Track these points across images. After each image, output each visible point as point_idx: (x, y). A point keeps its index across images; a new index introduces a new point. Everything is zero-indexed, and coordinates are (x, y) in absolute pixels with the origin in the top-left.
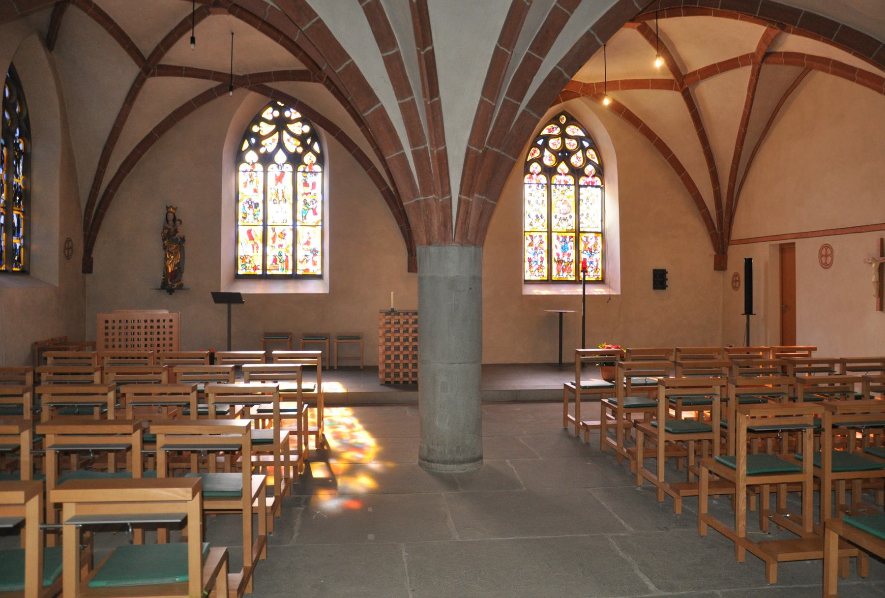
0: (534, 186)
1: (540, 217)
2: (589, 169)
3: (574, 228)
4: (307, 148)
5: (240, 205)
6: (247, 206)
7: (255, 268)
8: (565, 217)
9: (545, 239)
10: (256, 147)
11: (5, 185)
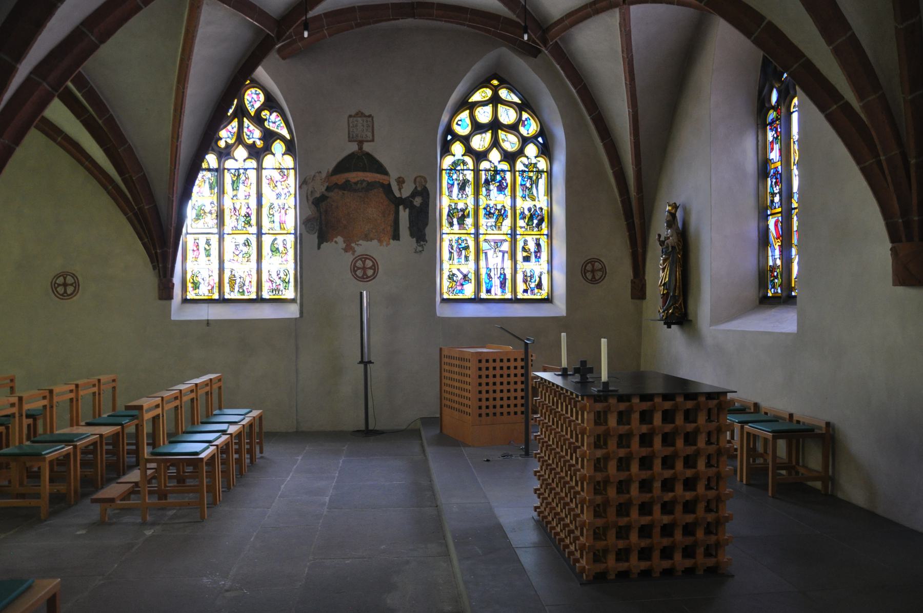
5: (769, 179)
6: (774, 180)
11: (509, 212)
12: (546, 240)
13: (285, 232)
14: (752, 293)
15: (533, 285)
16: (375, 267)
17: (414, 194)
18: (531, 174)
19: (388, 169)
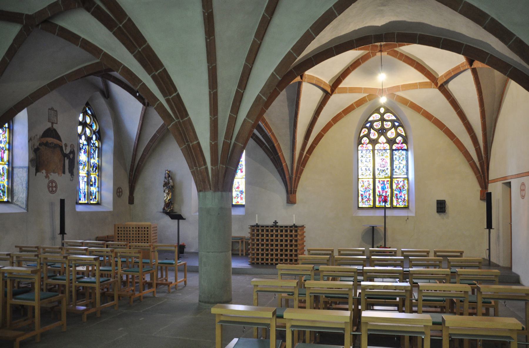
0: (364, 152)
1: (368, 170)
2: (399, 139)
3: (389, 175)
8: (384, 169)
9: (371, 183)
11: (87, 163)
12: (97, 177)
13: (4, 163)
15: (94, 197)
18: (94, 148)
19: (62, 139)
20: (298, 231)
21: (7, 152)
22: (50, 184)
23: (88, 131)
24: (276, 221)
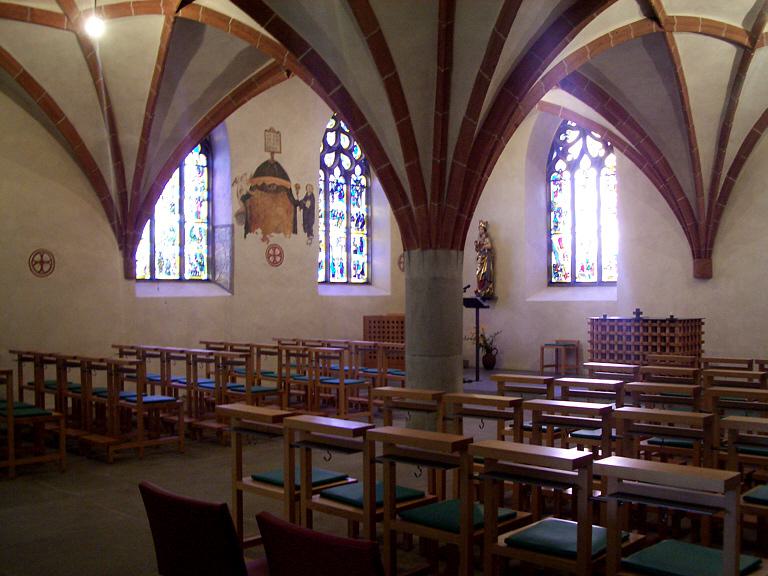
4: (609, 150)
5: (552, 214)
6: (558, 214)
7: (566, 276)
10: (563, 155)
14: (545, 281)
15: (359, 272)
16: (281, 255)
17: (306, 198)
20: (677, 329)
21: (205, 204)
22: (271, 252)
23: (346, 162)
24: (638, 310)
